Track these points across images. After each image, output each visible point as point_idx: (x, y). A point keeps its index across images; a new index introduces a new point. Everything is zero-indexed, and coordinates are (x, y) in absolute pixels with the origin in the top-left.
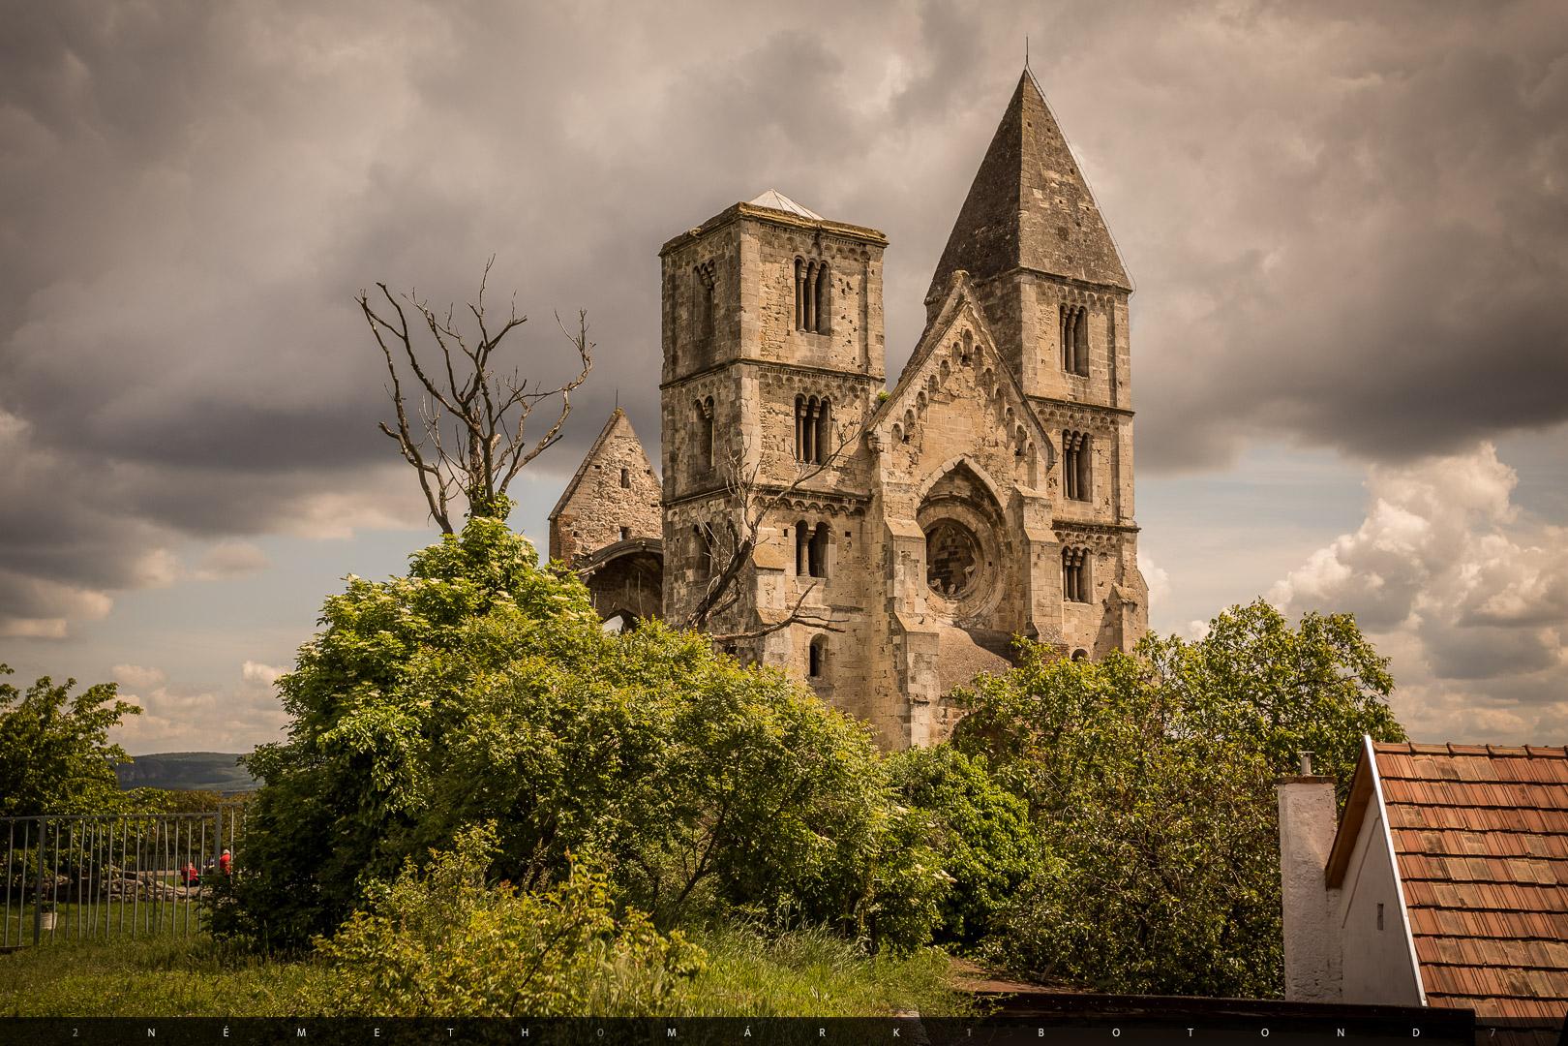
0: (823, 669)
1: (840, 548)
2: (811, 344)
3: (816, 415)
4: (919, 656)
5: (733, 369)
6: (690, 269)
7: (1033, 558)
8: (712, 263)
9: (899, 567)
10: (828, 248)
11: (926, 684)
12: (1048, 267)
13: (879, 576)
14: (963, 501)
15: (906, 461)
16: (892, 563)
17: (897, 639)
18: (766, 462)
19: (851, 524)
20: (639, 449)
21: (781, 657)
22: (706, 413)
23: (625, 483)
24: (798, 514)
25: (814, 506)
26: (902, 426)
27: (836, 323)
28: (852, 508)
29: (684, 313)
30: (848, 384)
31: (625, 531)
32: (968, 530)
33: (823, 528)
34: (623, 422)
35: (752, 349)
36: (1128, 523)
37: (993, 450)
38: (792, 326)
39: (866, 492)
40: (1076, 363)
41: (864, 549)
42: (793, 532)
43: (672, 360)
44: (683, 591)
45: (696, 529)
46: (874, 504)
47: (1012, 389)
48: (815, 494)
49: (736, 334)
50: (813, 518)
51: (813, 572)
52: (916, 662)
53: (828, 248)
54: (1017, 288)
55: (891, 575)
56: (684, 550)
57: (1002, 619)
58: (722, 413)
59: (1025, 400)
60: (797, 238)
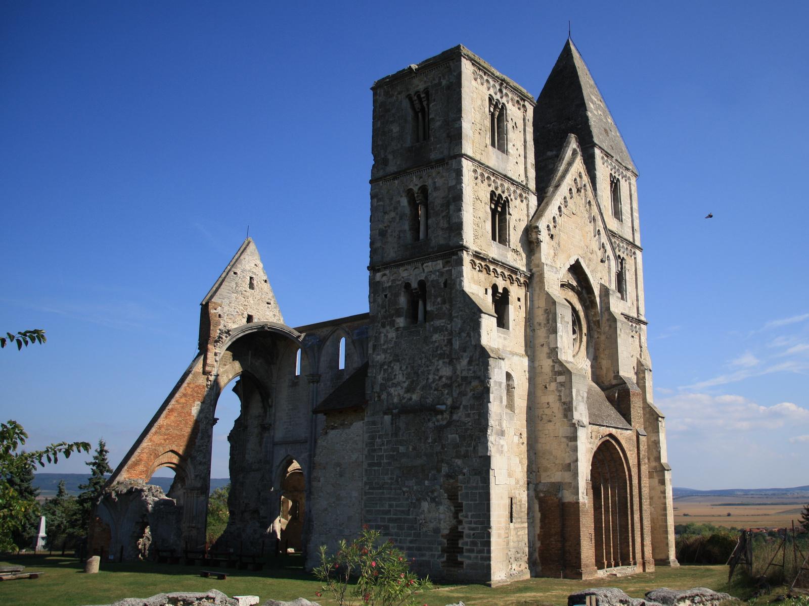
1: (515, 308)
3: (499, 209)
4: (578, 391)
6: (402, 97)
7: (618, 332)
9: (559, 325)
10: (507, 95)
11: (581, 413)
12: (605, 149)
14: (572, 288)
15: (552, 252)
17: (561, 379)
18: (476, 237)
20: (261, 265)
21: (500, 384)
22: (420, 198)
23: (251, 286)
25: (503, 275)
27: (511, 149)
28: (522, 280)
29: (395, 129)
30: (519, 192)
31: (250, 318)
33: (506, 290)
34: (252, 247)
35: (468, 148)
36: (642, 318)
38: (489, 142)
40: (617, 214)
42: (490, 291)
43: (380, 162)
44: (392, 334)
45: (407, 286)
46: (536, 279)
48: (504, 265)
49: (455, 136)
50: (501, 284)
52: (577, 395)
53: (507, 95)
55: (554, 331)
58: (437, 198)
59: (605, 228)
60: (492, 82)
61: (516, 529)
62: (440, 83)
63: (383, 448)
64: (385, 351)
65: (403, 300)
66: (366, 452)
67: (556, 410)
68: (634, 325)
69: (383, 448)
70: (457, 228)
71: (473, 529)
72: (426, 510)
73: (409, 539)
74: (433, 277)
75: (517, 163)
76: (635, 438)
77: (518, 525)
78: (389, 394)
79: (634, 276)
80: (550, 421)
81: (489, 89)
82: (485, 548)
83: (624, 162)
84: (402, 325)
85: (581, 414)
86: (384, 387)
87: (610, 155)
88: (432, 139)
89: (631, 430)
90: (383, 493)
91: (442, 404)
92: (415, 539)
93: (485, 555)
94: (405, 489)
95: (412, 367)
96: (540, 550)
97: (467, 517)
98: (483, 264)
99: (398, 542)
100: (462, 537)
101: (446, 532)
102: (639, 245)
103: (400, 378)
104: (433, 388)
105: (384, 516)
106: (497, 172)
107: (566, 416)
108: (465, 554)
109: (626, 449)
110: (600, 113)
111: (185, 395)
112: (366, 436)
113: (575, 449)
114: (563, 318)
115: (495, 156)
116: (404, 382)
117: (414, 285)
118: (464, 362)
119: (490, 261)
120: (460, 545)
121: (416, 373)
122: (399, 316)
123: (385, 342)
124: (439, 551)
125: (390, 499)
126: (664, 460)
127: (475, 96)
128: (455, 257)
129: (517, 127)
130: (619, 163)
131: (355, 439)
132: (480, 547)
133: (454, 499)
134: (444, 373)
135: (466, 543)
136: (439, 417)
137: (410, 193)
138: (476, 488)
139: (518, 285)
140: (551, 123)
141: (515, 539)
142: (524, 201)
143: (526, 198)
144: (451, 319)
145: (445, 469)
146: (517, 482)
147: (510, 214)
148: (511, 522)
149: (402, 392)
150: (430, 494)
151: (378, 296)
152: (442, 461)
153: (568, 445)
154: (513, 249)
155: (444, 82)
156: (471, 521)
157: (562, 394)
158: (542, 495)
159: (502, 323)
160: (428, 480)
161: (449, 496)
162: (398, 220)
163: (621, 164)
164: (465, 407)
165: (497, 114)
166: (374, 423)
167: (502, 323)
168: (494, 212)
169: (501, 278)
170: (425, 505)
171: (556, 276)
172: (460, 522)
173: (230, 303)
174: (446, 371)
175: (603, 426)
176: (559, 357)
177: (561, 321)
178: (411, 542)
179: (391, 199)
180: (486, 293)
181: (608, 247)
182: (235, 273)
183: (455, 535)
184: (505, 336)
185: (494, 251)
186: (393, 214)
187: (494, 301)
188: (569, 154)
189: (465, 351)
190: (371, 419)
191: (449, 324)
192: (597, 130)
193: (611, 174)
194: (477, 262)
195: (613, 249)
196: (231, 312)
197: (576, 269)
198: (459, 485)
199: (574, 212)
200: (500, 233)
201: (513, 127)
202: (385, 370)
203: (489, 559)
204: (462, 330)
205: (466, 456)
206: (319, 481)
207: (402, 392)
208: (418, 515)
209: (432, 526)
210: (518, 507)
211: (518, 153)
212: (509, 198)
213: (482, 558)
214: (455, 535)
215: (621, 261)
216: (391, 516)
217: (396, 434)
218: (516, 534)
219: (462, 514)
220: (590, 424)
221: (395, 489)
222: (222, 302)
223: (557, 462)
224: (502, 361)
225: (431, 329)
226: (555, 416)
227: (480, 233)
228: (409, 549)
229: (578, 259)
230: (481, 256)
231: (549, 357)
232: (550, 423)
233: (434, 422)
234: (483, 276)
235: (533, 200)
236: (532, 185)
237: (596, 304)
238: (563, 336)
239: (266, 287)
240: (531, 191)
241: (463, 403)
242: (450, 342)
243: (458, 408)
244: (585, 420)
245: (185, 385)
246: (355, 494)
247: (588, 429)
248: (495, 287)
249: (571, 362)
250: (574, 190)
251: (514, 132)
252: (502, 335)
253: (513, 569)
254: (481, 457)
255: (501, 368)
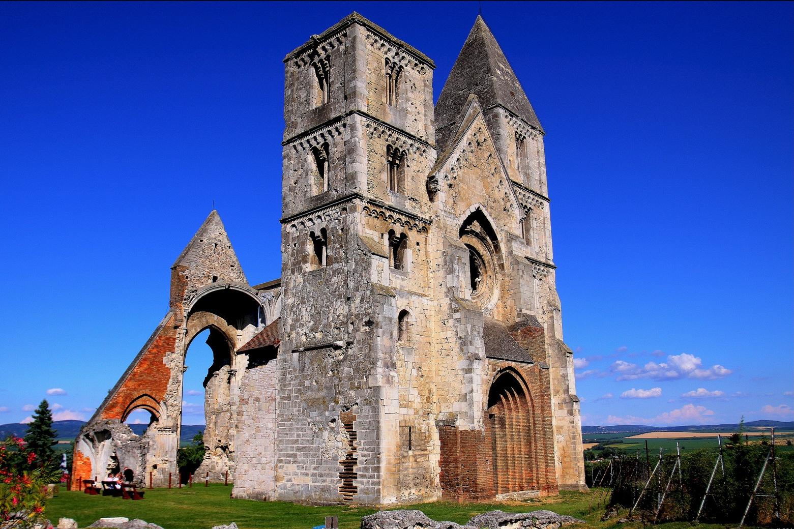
0: (404, 336)
2: (394, 114)
3: (397, 162)
4: (473, 327)
5: (349, 120)
8: (328, 58)
9: (455, 266)
10: (403, 58)
12: (510, 108)
13: (441, 273)
14: (476, 235)
15: (451, 201)
16: (451, 262)
17: (457, 315)
19: (421, 238)
21: (390, 319)
24: (391, 226)
26: (449, 177)
28: (421, 225)
29: (303, 95)
31: (215, 279)
32: (478, 254)
33: (404, 236)
36: (551, 263)
37: (493, 205)
39: (428, 218)
41: (427, 255)
42: (386, 236)
44: (300, 279)
45: (312, 234)
46: (434, 225)
47: (502, 169)
48: (400, 212)
49: (350, 95)
50: (398, 229)
51: (396, 267)
52: (472, 331)
54: (496, 116)
55: (451, 271)
56: (301, 250)
57: (498, 312)
58: (336, 152)
60: (387, 45)
61: (414, 456)
62: (339, 49)
63: (292, 382)
64: (294, 295)
65: (310, 248)
66: (278, 387)
67: (453, 345)
68: (542, 269)
69: (292, 382)
70: (351, 178)
71: (365, 456)
72: (327, 439)
73: (312, 466)
74: (332, 225)
75: (416, 120)
76: (537, 372)
77: (416, 453)
78: (298, 333)
79: (542, 225)
80: (448, 355)
81: (386, 53)
82: (376, 474)
83: (530, 122)
84: (308, 270)
85: (477, 348)
86: (293, 327)
87: (515, 114)
88: (332, 99)
89: (533, 363)
90: (292, 424)
91: (340, 340)
92: (318, 466)
93: (376, 480)
94: (309, 420)
95: (316, 308)
96: (440, 476)
97: (360, 444)
98: (378, 210)
99: (304, 469)
100: (356, 463)
101: (343, 459)
102: (547, 197)
103: (306, 318)
104: (333, 326)
105: (293, 446)
106: (393, 127)
107: (462, 350)
108: (358, 479)
109: (527, 381)
110: (506, 78)
111: (156, 346)
112: (279, 374)
113: (471, 381)
114: (459, 259)
115: (392, 113)
116: (309, 322)
117: (318, 233)
118: (358, 301)
119: (386, 208)
120: (354, 471)
121: (319, 313)
122: (306, 262)
123: (294, 287)
124: (337, 477)
125: (298, 429)
126: (573, 392)
127: (370, 58)
128: (351, 205)
129: (415, 88)
130: (525, 122)
131: (270, 376)
132: (371, 473)
133: (349, 428)
134: (342, 312)
135: (360, 469)
136: (337, 352)
137: (315, 151)
138: (367, 417)
139: (417, 231)
140: (462, 90)
141: (414, 466)
142: (424, 154)
143: (424, 151)
144: (347, 262)
145: (342, 401)
146: (416, 413)
147: (408, 166)
148: (410, 450)
149: (307, 331)
150: (330, 423)
151: (289, 246)
152: (340, 393)
153: (464, 377)
154: (412, 198)
155: (342, 48)
156: (364, 448)
157: (458, 329)
158: (441, 424)
159: (398, 263)
160: (328, 411)
161: (345, 425)
162: (304, 175)
163: (527, 123)
164: (358, 342)
165: (394, 75)
166: (285, 361)
167: (398, 263)
168: (392, 164)
169: (398, 224)
170: (326, 434)
171: (455, 222)
172: (354, 449)
173: (197, 266)
174: (343, 310)
175: (503, 359)
176: (456, 295)
177: (458, 262)
178: (314, 469)
179: (299, 158)
180: (382, 238)
181: (512, 197)
182: (201, 241)
183: (350, 462)
184: (403, 277)
185: (391, 200)
186: (300, 172)
187: (391, 244)
188: (471, 111)
189: (357, 290)
190: (282, 357)
191: (345, 267)
192: (502, 92)
193: (516, 132)
194: (372, 208)
195: (517, 198)
196: (198, 274)
197: (477, 215)
198: (353, 414)
199: (475, 164)
200: (396, 184)
201: (412, 87)
202: (295, 313)
203: (379, 483)
204: (355, 271)
205: (358, 388)
206: (243, 415)
207: (307, 331)
208: (319, 444)
209: (332, 453)
210: (417, 435)
211: (417, 110)
212: (407, 152)
213: (373, 483)
214: (350, 462)
215: (527, 211)
216: (299, 445)
217: (302, 370)
218: (416, 460)
219: (356, 442)
220: (487, 357)
221: (302, 420)
222: (190, 265)
223: (455, 393)
224: (393, 300)
225: (331, 273)
226: (452, 350)
227: (375, 183)
228: (313, 475)
229: (479, 207)
230: (377, 203)
231: (447, 296)
232: (448, 357)
233: (333, 357)
234: (378, 222)
235: (433, 154)
236: (432, 141)
237: (500, 248)
238: (460, 275)
239: (231, 252)
240: (430, 145)
241: (358, 338)
242: (346, 282)
243: (352, 343)
244: (482, 353)
245: (157, 337)
246: (270, 426)
247: (484, 362)
248: (391, 233)
249: (467, 300)
250: (474, 145)
251: (413, 92)
252: (400, 276)
253: (412, 494)
254: (371, 388)
255: (391, 304)
